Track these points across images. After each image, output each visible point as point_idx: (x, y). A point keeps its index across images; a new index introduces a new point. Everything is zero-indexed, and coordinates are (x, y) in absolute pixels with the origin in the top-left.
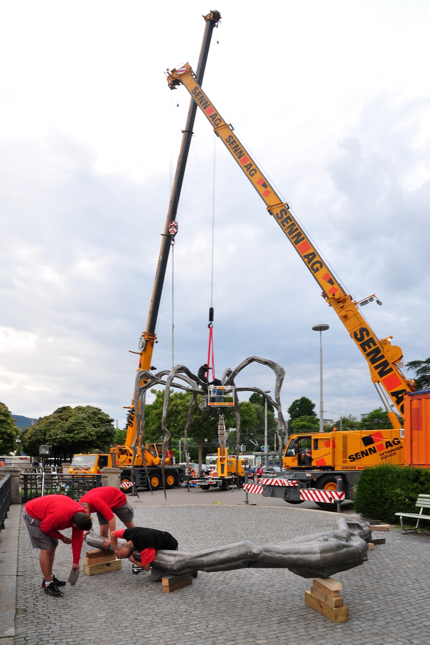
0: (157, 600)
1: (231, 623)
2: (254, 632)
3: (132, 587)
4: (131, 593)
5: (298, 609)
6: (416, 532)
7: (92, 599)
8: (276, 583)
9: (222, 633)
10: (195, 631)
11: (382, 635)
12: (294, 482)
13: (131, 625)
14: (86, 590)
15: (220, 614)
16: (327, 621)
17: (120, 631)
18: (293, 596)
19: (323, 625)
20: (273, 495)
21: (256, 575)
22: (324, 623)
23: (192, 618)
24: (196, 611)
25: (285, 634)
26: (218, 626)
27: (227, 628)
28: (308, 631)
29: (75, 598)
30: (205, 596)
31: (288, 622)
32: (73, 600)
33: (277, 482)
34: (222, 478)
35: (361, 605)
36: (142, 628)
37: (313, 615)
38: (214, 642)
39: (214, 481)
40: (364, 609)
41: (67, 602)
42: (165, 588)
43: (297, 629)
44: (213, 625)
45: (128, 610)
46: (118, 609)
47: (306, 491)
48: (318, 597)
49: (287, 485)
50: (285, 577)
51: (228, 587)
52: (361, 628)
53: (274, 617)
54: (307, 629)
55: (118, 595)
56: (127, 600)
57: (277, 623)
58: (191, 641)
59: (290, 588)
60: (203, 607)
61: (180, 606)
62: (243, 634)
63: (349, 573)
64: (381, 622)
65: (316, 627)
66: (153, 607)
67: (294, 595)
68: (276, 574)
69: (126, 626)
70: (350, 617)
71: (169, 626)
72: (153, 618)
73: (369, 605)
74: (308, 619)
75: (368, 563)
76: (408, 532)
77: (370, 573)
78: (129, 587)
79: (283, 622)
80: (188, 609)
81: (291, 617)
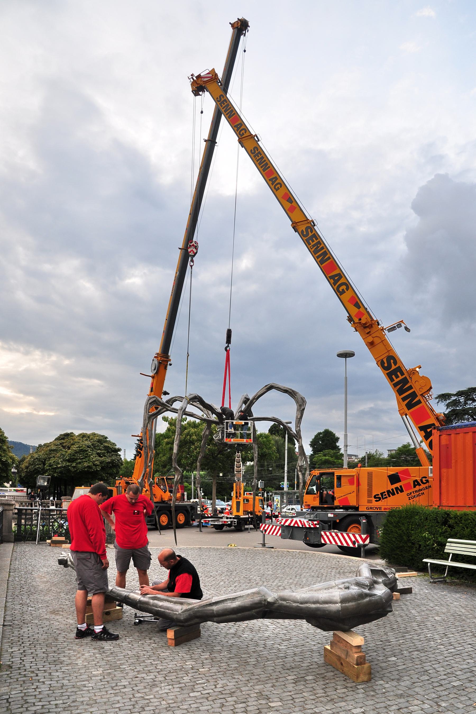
0: (160, 655)
1: (242, 682)
2: (268, 693)
3: (134, 639)
4: (132, 647)
5: (317, 666)
7: (88, 653)
8: (293, 637)
9: (232, 694)
10: (202, 692)
11: (407, 696)
13: (130, 684)
14: (82, 643)
15: (231, 672)
16: (348, 681)
17: (117, 691)
18: (311, 652)
19: (344, 685)
20: (292, 537)
21: (272, 627)
22: (345, 683)
23: (199, 676)
24: (204, 668)
25: (301, 695)
26: (228, 685)
27: (237, 688)
28: (326, 692)
29: (69, 652)
30: (214, 651)
31: (305, 681)
32: (66, 654)
35: (385, 662)
36: (142, 687)
37: (332, 674)
38: (223, 704)
40: (388, 667)
41: (59, 656)
42: (170, 641)
43: (314, 690)
44: (222, 684)
45: (128, 666)
46: (116, 665)
48: (339, 653)
50: (303, 630)
51: (240, 640)
52: (385, 688)
53: (289, 675)
54: (327, 690)
55: (118, 649)
56: (127, 654)
57: (293, 683)
58: (197, 703)
59: (308, 642)
60: (212, 663)
61: (186, 662)
62: (255, 695)
63: (372, 626)
64: (406, 682)
65: (335, 687)
66: (156, 663)
67: (312, 651)
68: (293, 626)
69: (124, 686)
70: (373, 676)
71: (172, 685)
72: (155, 676)
73: (393, 662)
74: (327, 678)
75: (393, 614)
77: (395, 627)
78: (130, 640)
79: (300, 681)
80: (195, 665)
81: (308, 676)
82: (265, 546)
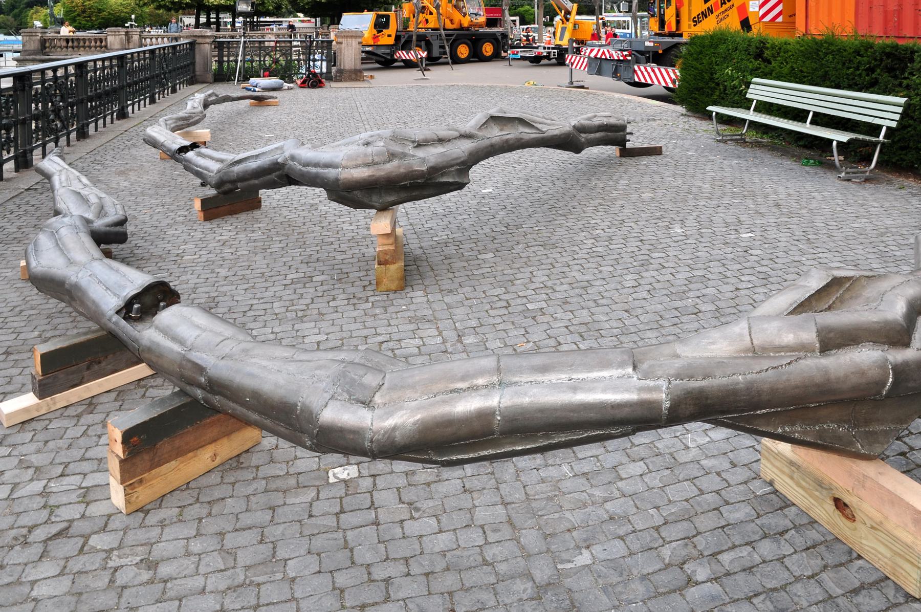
6: (744, 140)
12: (625, 53)
20: (599, 73)
33: (604, 53)
34: (558, 47)
39: (547, 50)
47: (642, 68)
49: (616, 58)
76: (729, 138)
82: (572, 83)
